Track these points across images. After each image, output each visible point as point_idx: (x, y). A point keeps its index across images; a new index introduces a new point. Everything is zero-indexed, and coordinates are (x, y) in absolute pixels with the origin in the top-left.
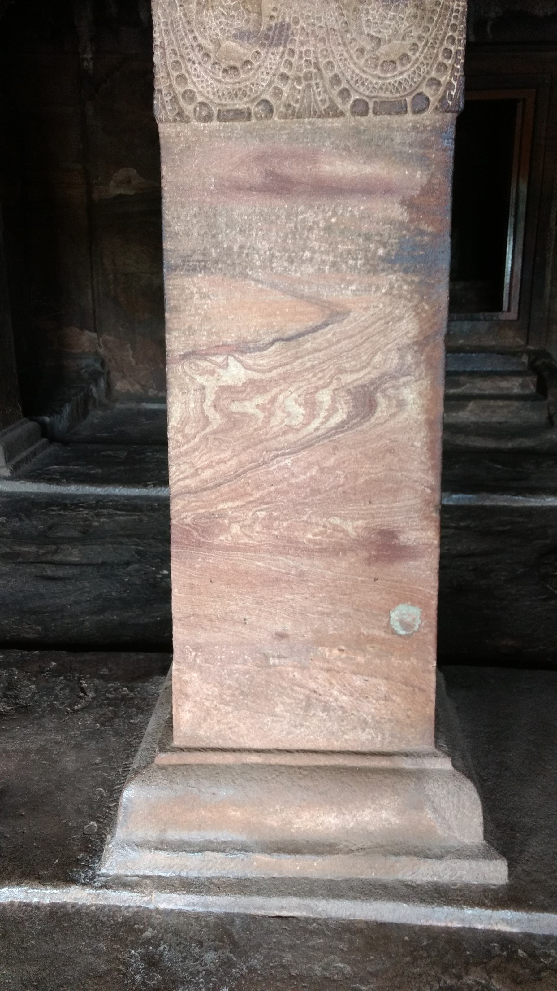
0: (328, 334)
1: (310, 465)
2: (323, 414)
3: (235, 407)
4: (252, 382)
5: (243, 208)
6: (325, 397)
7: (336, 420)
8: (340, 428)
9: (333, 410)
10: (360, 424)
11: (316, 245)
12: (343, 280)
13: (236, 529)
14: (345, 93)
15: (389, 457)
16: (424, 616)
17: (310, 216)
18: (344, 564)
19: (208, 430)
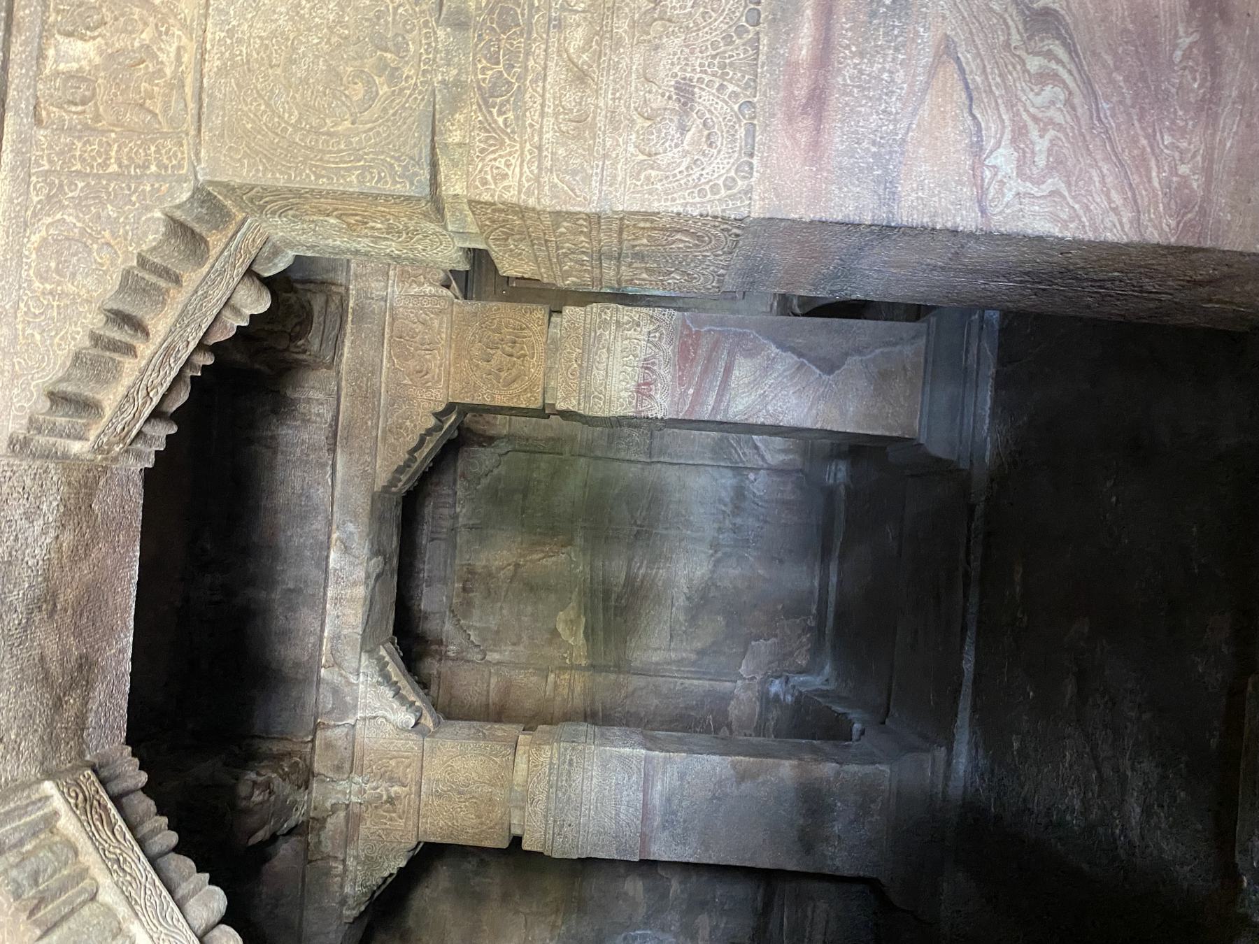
0: (966, 56)
1: (1112, 81)
2: (1053, 65)
3: (1041, 161)
4: (1013, 141)
5: (836, 140)
6: (1034, 64)
7: (1061, 52)
9: (1050, 55)
10: (1066, 27)
11: (877, 66)
12: (913, 40)
13: (1184, 169)
14: (740, 31)
18: (1230, 50)
19: (1066, 194)
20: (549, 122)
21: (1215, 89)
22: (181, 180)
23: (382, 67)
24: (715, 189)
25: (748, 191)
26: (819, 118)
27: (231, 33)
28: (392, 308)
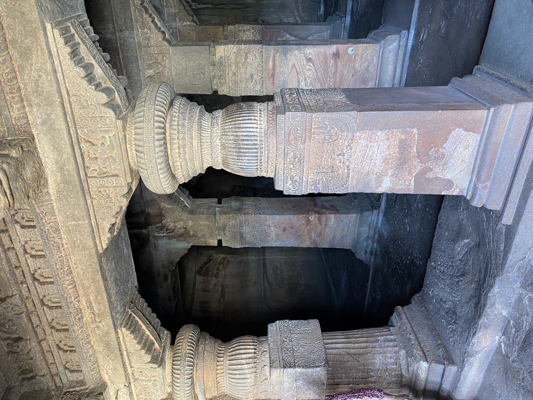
0: (297, 67)
3: (309, 84)
5: (277, 82)
6: (308, 67)
7: (312, 65)
8: (313, 65)
13: (331, 84)
17: (278, 70)
25: (263, 92)
26: (274, 78)
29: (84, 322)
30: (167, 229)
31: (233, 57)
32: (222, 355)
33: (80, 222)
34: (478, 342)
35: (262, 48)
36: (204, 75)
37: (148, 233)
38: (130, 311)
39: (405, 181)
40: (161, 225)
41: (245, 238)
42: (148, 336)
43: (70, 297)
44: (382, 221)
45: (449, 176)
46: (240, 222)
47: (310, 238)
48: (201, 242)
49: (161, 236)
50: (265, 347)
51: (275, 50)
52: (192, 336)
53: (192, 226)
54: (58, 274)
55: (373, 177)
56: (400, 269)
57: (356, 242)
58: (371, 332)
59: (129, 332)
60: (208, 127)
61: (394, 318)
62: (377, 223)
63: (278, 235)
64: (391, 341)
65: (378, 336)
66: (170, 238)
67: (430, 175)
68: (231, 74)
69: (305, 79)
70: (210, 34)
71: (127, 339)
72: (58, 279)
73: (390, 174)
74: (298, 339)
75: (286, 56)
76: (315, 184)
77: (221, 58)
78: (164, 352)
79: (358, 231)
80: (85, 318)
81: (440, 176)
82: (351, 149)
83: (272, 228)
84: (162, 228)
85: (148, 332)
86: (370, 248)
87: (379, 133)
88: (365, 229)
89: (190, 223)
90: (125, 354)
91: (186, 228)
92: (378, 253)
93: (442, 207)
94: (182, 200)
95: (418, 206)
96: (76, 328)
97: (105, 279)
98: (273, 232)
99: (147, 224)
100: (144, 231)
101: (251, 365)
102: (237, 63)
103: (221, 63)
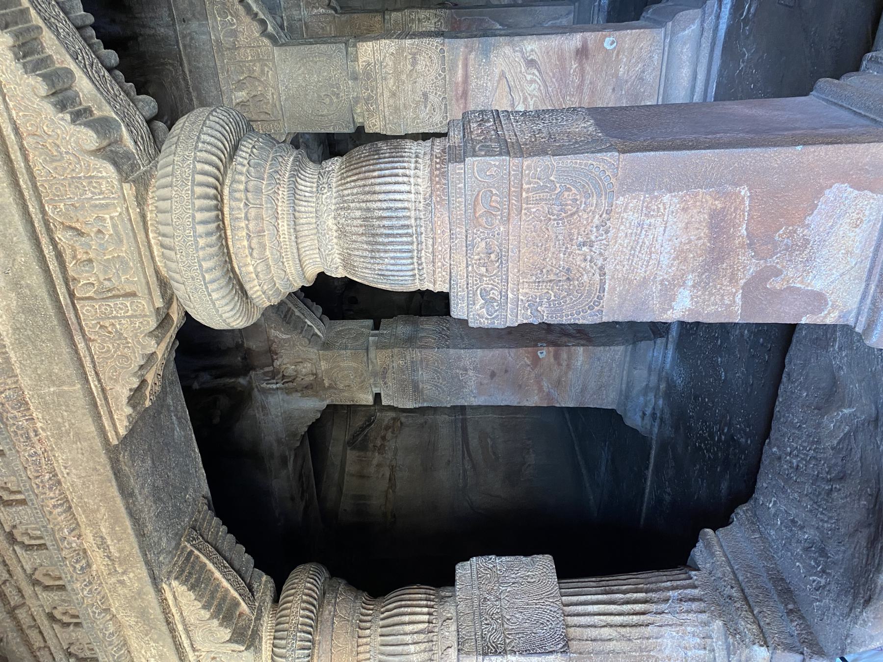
6: (529, 77)
15: (550, 53)
16: (610, 36)
20: (386, 109)
21: (583, 81)
22: (282, 134)
23: (334, 94)
24: (437, 124)
26: (466, 100)
27: (286, 87)
28: (305, 23)
29: (94, 574)
30: (283, 376)
31: (390, 63)
32: (368, 624)
33: (65, 388)
34: (874, 618)
35: (443, 44)
36: (337, 98)
37: (250, 383)
38: (188, 545)
39: (722, 296)
40: (271, 368)
41: (422, 392)
42: (227, 590)
43: (61, 529)
44: (673, 358)
45: (817, 285)
46: (412, 362)
47: (540, 389)
48: (342, 399)
49: (273, 389)
50: (449, 610)
51: (466, 47)
52: (310, 589)
53: (327, 371)
54: (31, 486)
55: (656, 288)
56: (708, 451)
57: (626, 396)
58: (653, 579)
59: (185, 588)
60: (311, 192)
61: (698, 553)
62: (664, 362)
63: (481, 384)
64: (693, 600)
65: (668, 589)
66: (289, 391)
67: (776, 284)
68: (387, 94)
69: (525, 99)
70: (359, 28)
71: (183, 601)
72: (33, 497)
73: (690, 283)
74: (513, 595)
75: (487, 57)
76: (532, 304)
77: (369, 64)
78: (259, 618)
79: (628, 377)
80: (94, 567)
81: (799, 285)
82: (607, 232)
83: (471, 373)
84: (274, 375)
85: (225, 584)
86: (651, 407)
87: (666, 198)
88: (641, 375)
89: (324, 365)
90: (180, 627)
91: (316, 374)
92: (667, 416)
93: (794, 340)
94: (309, 323)
95: (742, 335)
96: (78, 585)
97: (126, 493)
98: (472, 379)
99: (247, 368)
100: (242, 381)
101: (423, 646)
102: (397, 74)
103: (368, 74)
